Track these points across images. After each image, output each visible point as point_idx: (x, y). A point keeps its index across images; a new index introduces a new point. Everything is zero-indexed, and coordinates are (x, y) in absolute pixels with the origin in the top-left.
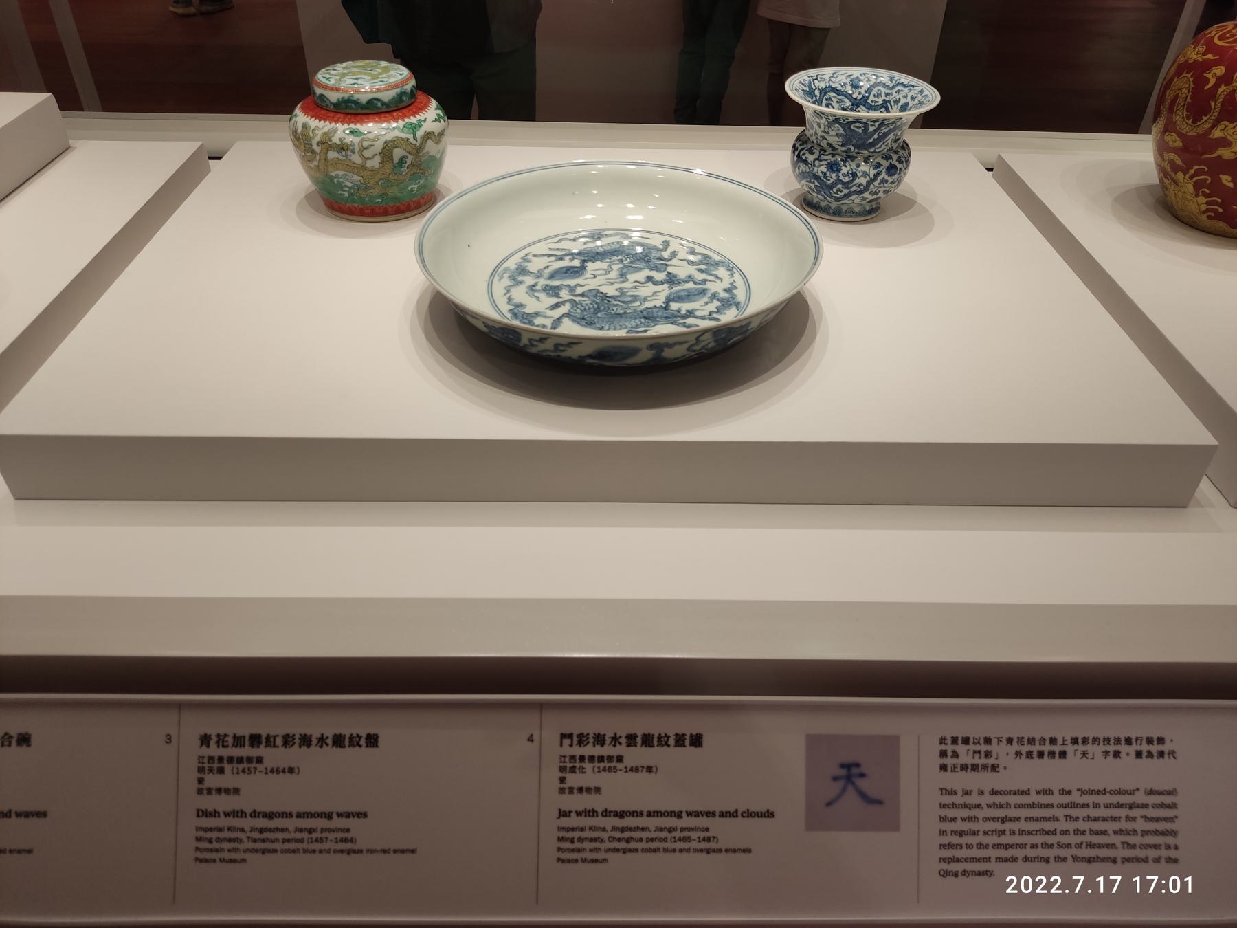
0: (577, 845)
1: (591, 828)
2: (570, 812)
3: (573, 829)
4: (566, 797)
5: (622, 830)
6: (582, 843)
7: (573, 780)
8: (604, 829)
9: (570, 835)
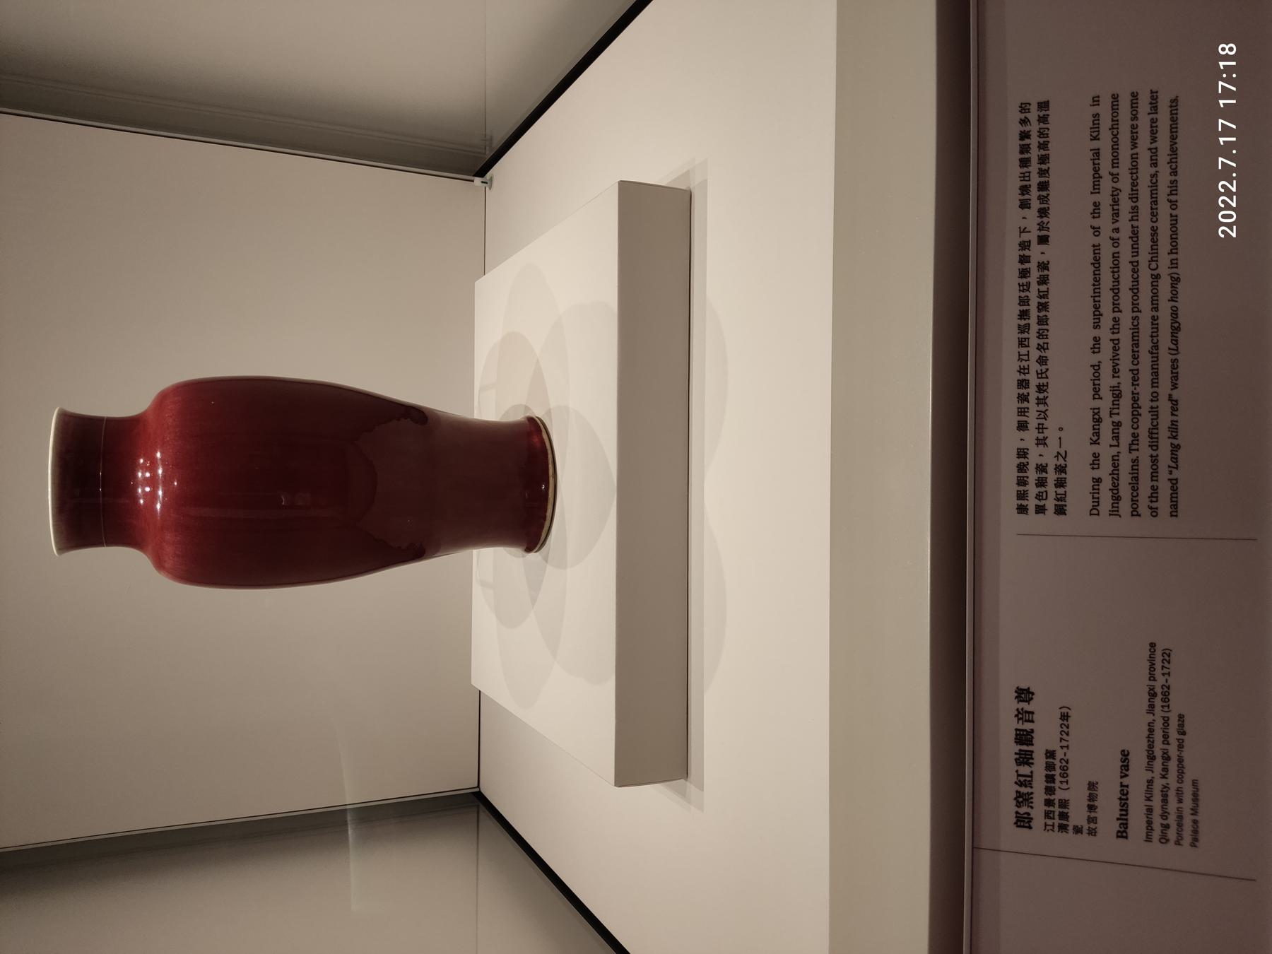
0: (1172, 820)
1: (1148, 799)
2: (1122, 785)
3: (1149, 823)
5: (1151, 758)
6: (1169, 814)
7: (1078, 815)
8: (1150, 782)
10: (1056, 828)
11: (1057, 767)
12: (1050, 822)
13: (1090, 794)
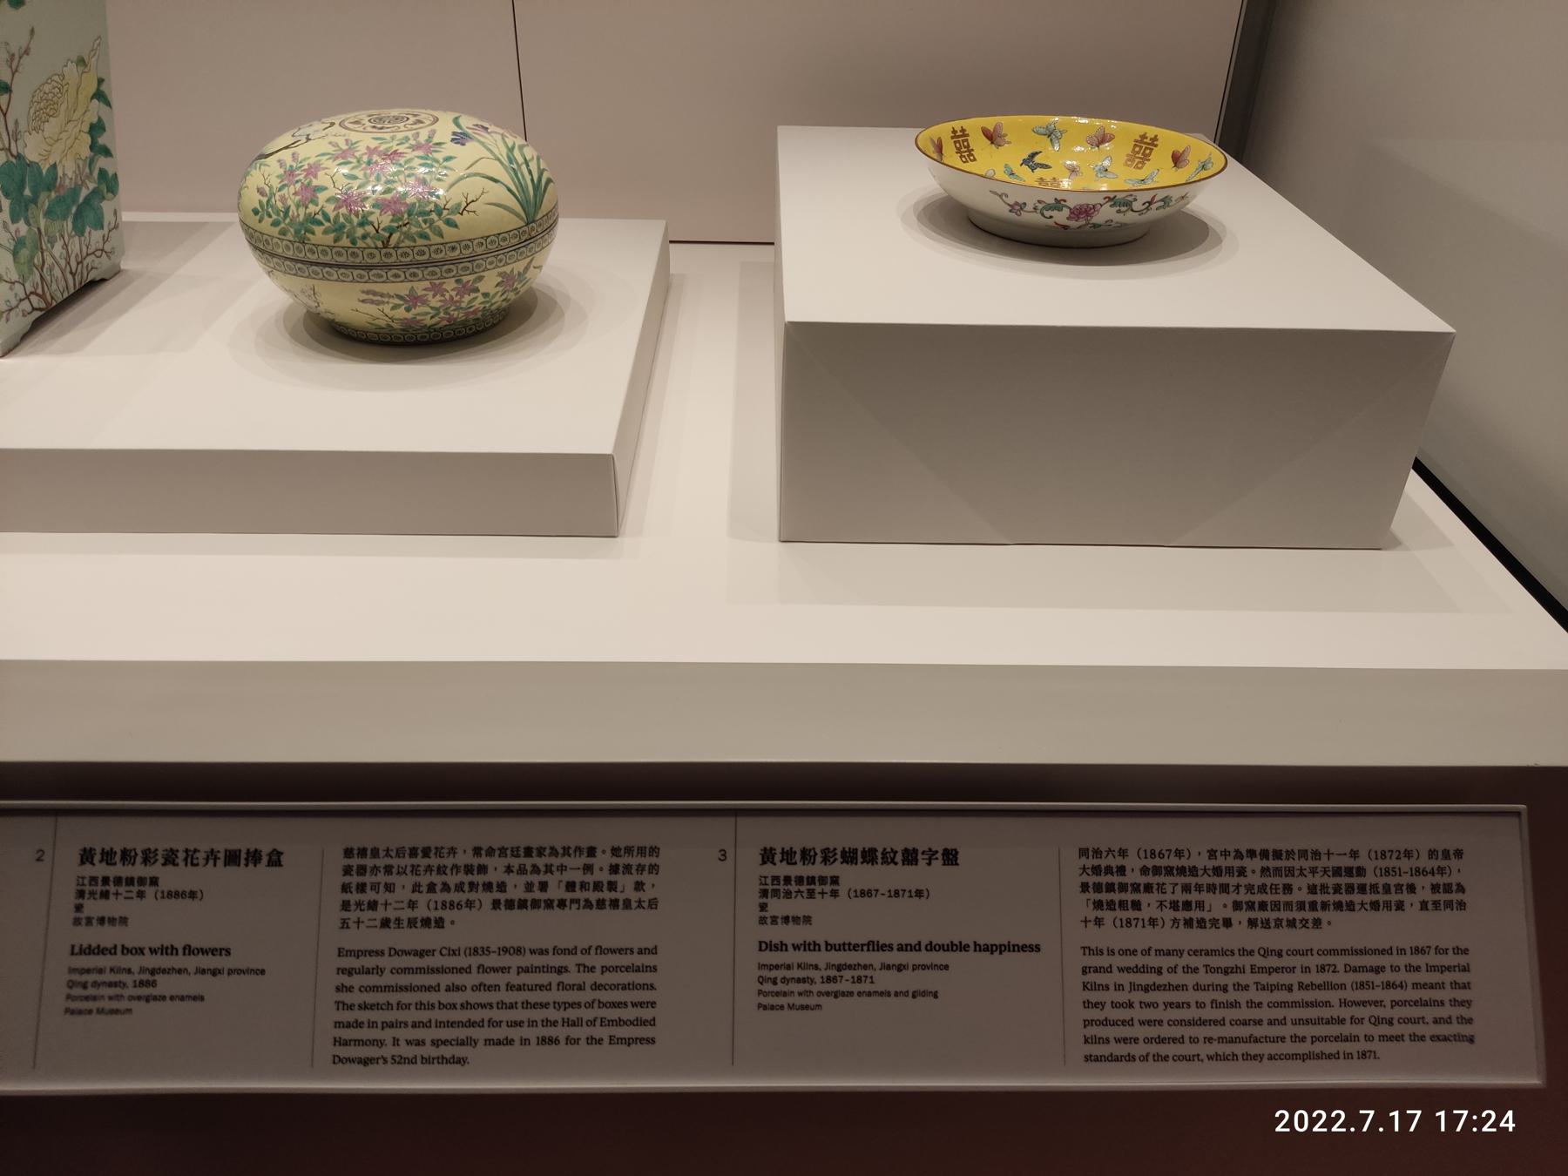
0: (781, 987)
1: (799, 966)
3: (777, 967)
7: (777, 907)
9: (773, 974)
10: (762, 887)
12: (769, 881)
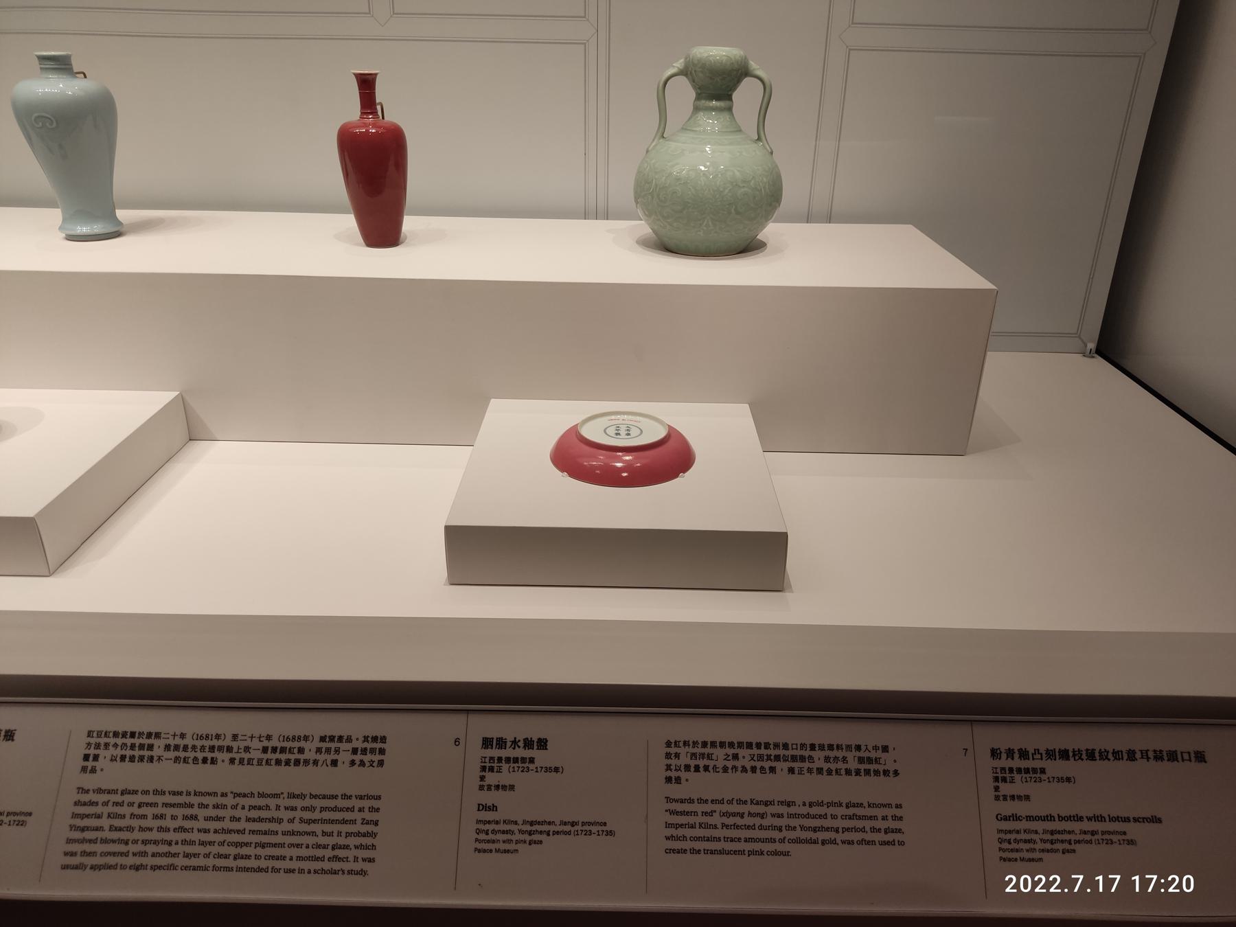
0: (491, 836)
1: (504, 822)
3: (489, 822)
4: (485, 793)
5: (532, 823)
7: (491, 778)
8: (516, 823)
11: (523, 765)
12: (487, 760)
13: (506, 786)
